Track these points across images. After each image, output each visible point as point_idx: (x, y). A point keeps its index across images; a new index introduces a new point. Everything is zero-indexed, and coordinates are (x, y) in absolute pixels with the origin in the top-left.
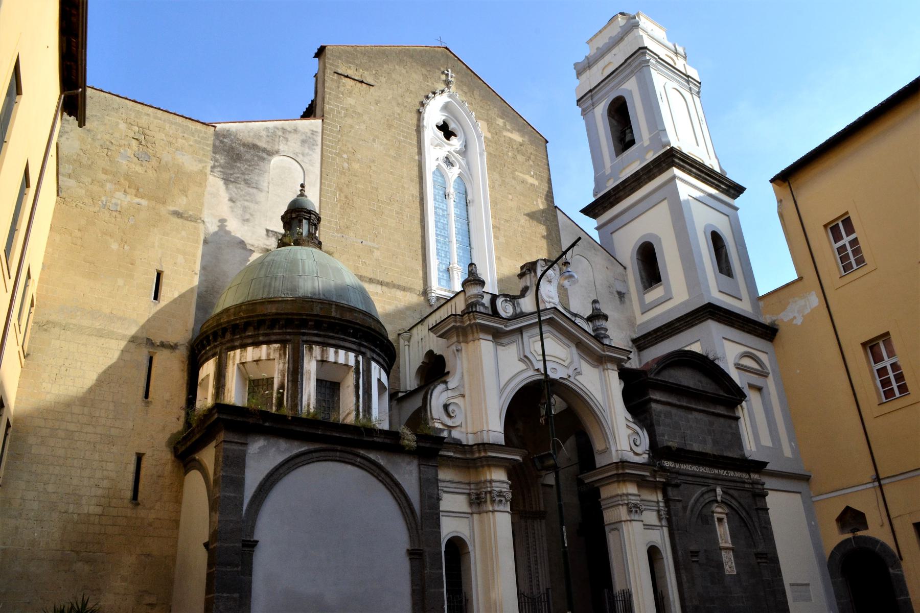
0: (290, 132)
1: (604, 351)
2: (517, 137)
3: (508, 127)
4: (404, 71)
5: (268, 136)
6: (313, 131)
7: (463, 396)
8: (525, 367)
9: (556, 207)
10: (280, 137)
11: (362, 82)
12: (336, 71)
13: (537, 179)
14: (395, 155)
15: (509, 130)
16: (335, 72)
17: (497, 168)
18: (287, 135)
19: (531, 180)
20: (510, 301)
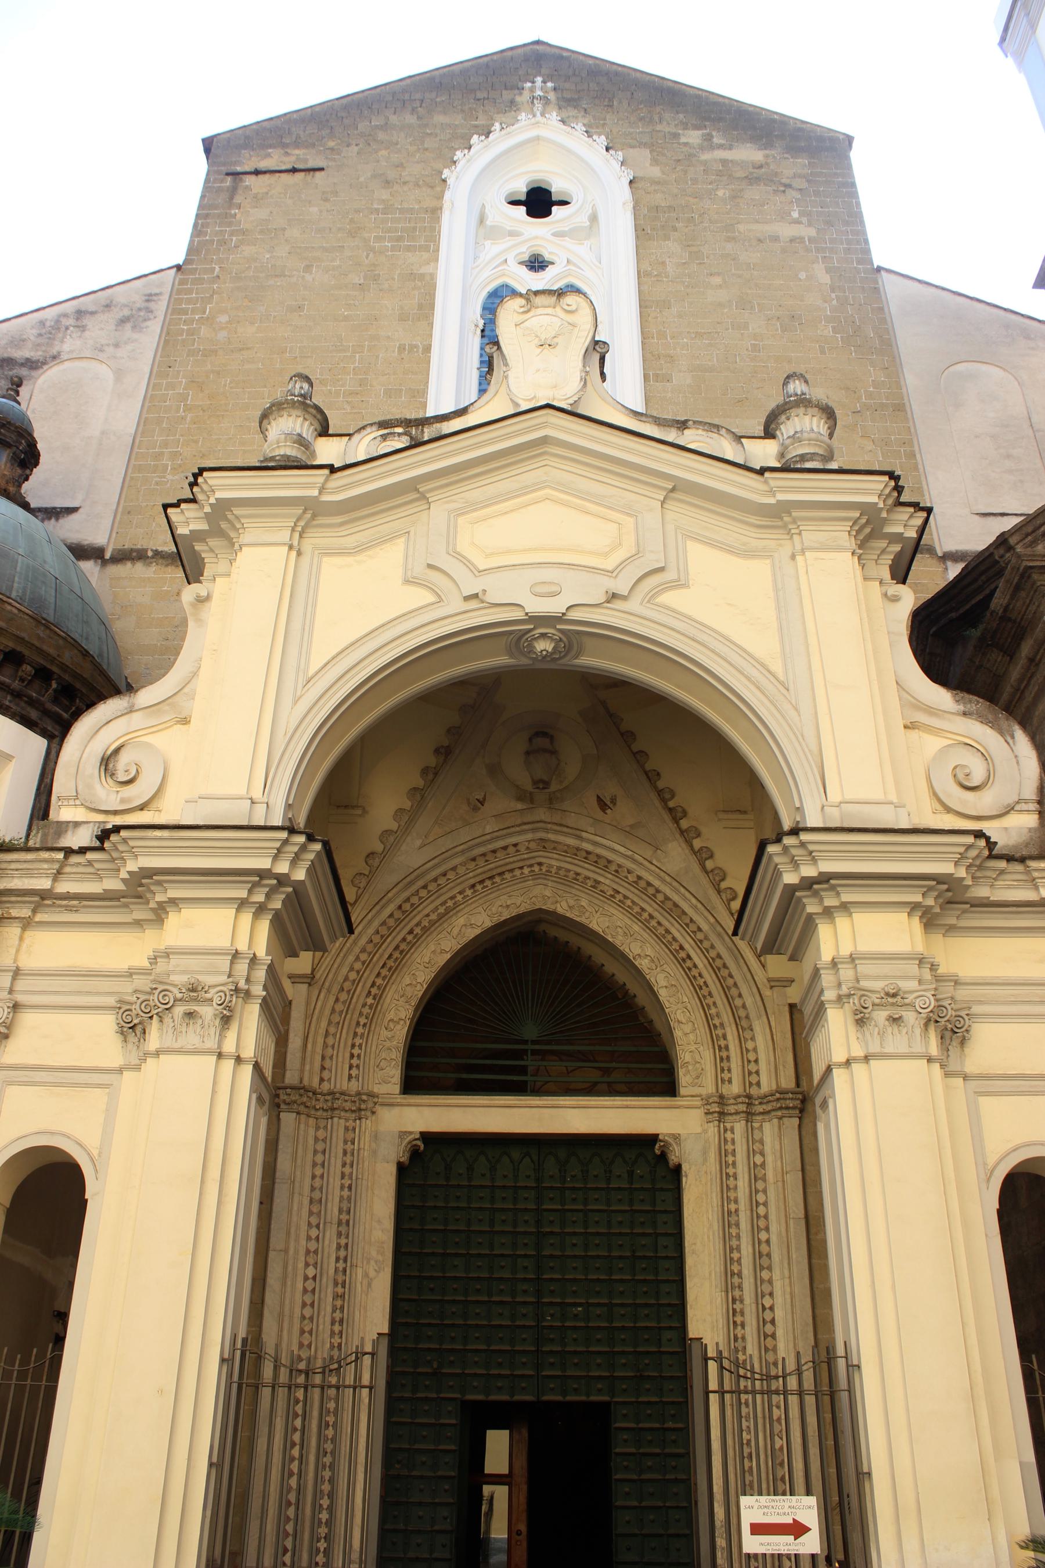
0: (92, 313)
1: (772, 492)
2: (748, 154)
3: (717, 140)
4: (410, 119)
5: (40, 335)
6: (150, 295)
7: (185, 721)
8: (431, 598)
9: (879, 269)
10: (67, 328)
11: (294, 170)
12: (230, 171)
13: (810, 225)
14: (362, 281)
15: (721, 147)
16: (228, 174)
17: (675, 229)
18: (87, 321)
19: (786, 231)
20: (405, 434)
